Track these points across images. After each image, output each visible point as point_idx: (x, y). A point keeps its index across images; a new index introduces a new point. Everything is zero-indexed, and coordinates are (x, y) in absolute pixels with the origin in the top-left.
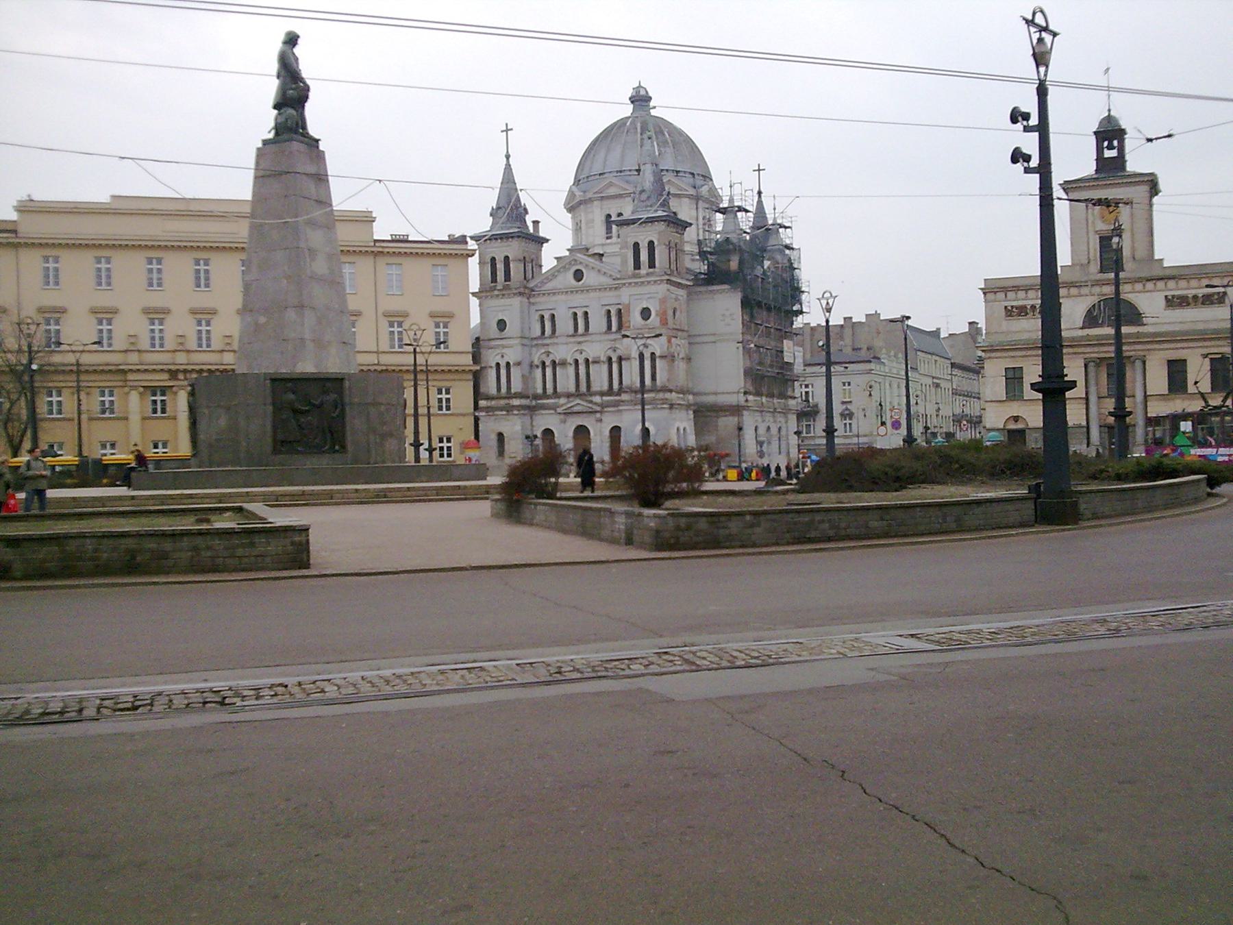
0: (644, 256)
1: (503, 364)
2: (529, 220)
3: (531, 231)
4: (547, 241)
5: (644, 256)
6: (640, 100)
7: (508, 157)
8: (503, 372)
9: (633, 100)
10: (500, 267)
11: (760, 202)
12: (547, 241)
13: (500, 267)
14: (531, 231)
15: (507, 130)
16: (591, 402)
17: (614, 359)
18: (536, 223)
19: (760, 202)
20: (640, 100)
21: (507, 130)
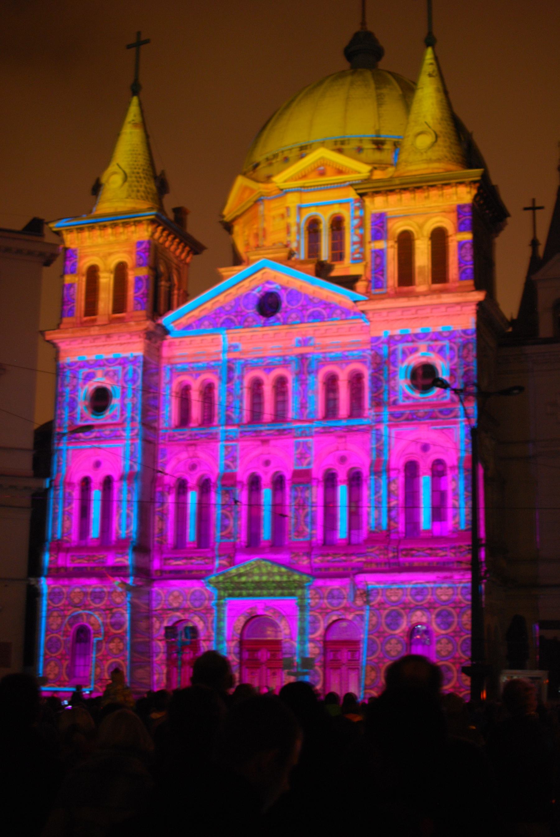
21: (139, 43)
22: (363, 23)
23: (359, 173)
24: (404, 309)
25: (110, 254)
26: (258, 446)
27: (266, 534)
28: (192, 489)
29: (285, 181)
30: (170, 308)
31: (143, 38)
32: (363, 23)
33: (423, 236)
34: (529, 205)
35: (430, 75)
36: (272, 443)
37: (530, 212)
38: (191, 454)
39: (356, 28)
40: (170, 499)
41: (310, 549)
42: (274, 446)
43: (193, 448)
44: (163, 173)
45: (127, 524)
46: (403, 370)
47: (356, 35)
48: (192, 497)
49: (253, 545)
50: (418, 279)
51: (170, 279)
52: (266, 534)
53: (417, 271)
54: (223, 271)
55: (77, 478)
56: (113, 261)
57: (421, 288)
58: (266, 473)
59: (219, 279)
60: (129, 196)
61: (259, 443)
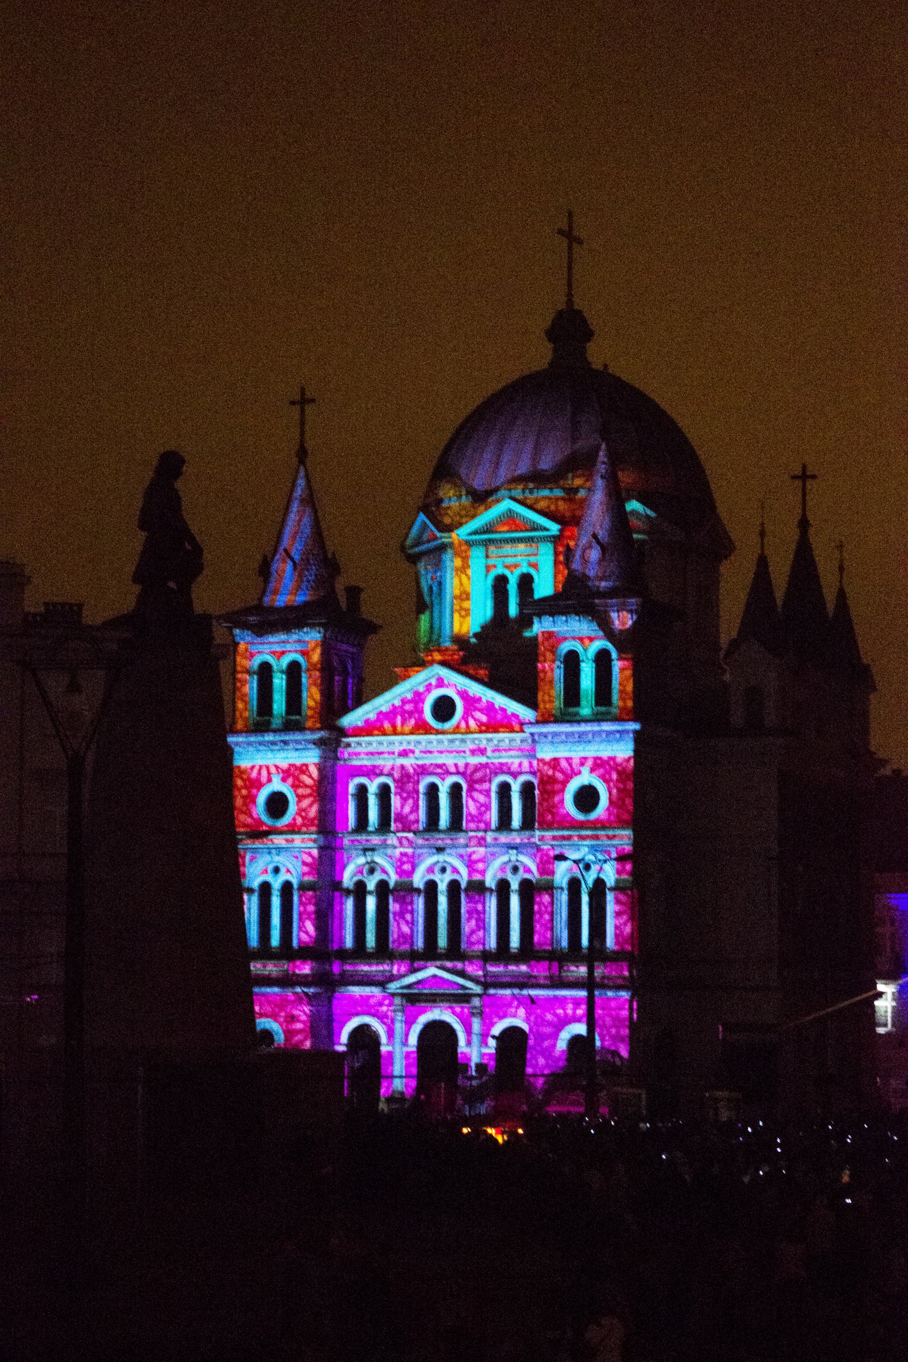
1: (276, 884)
2: (340, 586)
4: (373, 628)
6: (570, 330)
7: (302, 454)
8: (276, 902)
9: (552, 334)
10: (279, 682)
12: (373, 628)
13: (279, 682)
15: (303, 401)
16: (462, 974)
17: (515, 885)
18: (354, 592)
20: (570, 330)
21: (303, 401)
22: (570, 295)
23: (547, 530)
24: (568, 734)
25: (283, 653)
26: (434, 854)
27: (442, 941)
28: (370, 893)
29: (470, 534)
30: (346, 710)
31: (308, 395)
32: (570, 295)
33: (587, 658)
35: (602, 477)
36: (448, 851)
37: (798, 483)
38: (369, 859)
40: (349, 905)
41: (487, 957)
43: (370, 853)
45: (305, 931)
46: (573, 786)
47: (560, 313)
48: (371, 903)
49: (430, 953)
50: (583, 702)
51: (345, 672)
52: (442, 941)
55: (255, 884)
56: (285, 661)
57: (586, 710)
58: (442, 881)
60: (298, 588)
61: (435, 851)
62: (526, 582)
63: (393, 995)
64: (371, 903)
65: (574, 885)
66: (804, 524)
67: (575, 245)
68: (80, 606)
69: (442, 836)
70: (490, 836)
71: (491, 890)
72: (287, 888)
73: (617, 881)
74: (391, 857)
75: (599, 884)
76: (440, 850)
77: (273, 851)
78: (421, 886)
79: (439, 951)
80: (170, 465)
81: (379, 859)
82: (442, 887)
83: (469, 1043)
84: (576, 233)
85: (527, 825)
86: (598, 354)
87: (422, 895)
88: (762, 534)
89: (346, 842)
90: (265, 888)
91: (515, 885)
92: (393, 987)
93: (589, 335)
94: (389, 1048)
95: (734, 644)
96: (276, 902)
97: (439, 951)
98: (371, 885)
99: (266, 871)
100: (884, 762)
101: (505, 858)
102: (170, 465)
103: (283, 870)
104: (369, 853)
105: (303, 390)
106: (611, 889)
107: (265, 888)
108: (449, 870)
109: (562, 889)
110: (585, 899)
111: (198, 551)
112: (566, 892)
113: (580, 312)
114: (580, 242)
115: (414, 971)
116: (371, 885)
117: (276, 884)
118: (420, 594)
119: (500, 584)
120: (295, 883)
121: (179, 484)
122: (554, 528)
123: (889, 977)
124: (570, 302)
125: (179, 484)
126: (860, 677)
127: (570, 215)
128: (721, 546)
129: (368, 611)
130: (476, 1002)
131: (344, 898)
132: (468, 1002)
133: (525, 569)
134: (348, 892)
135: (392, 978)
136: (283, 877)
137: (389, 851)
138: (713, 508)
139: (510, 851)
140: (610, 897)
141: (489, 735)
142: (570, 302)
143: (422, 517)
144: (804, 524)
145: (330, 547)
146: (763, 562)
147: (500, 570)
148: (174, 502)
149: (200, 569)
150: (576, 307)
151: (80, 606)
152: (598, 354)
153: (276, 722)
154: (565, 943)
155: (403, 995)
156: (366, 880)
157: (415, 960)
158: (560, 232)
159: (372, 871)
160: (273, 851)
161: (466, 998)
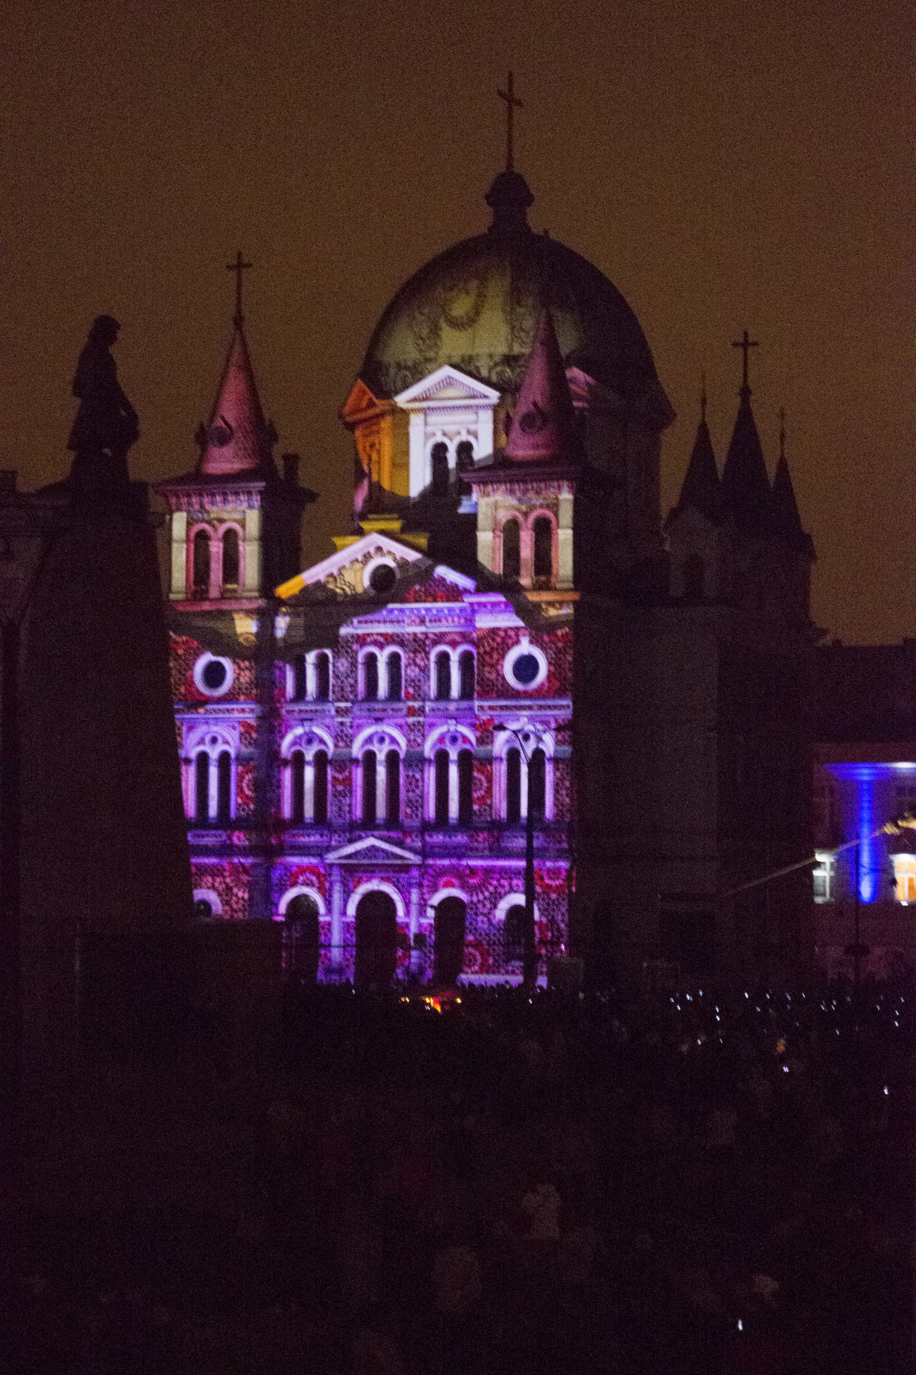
0: (527, 552)
1: (214, 753)
2: (277, 452)
3: (281, 473)
4: (312, 496)
5: (527, 552)
6: (510, 193)
8: (213, 772)
9: (492, 198)
10: (216, 548)
11: (745, 418)
12: (312, 496)
13: (216, 548)
14: (281, 473)
15: (240, 266)
16: (400, 844)
17: (453, 755)
18: (292, 460)
19: (745, 418)
20: (510, 193)
21: (240, 266)
22: (510, 157)
23: (486, 397)
27: (381, 811)
28: (309, 763)
29: (409, 401)
31: (246, 260)
32: (510, 157)
34: (741, 340)
38: (307, 729)
39: (501, 167)
40: (287, 775)
41: (426, 828)
42: (388, 725)
43: (309, 723)
44: (271, 425)
46: (513, 655)
48: (309, 773)
49: (368, 824)
52: (381, 811)
53: (522, 563)
54: (338, 541)
55: (193, 754)
58: (380, 751)
59: (332, 550)
61: (373, 721)
62: (465, 449)
63: (331, 866)
64: (309, 773)
65: (513, 756)
66: (745, 392)
67: (515, 107)
68: (14, 473)
69: (380, 706)
70: (428, 706)
71: (430, 761)
72: (224, 758)
73: (556, 751)
74: (328, 727)
75: (538, 754)
76: (378, 720)
77: (212, 722)
78: (360, 756)
79: (378, 821)
80: (105, 330)
81: (318, 731)
82: (381, 757)
83: (408, 913)
84: (517, 96)
85: (466, 694)
86: (537, 219)
87: (361, 764)
88: (704, 402)
89: (283, 712)
90: (203, 758)
91: (453, 755)
92: (331, 857)
93: (529, 199)
94: (327, 919)
95: (675, 513)
96: (213, 772)
97: (378, 821)
98: (309, 756)
99: (201, 741)
100: (824, 632)
101: (444, 729)
102: (105, 330)
103: (220, 740)
104: (307, 724)
105: (239, 254)
106: (550, 759)
107: (203, 758)
108: (387, 740)
109: (501, 759)
110: (524, 769)
111: (133, 418)
112: (505, 762)
113: (520, 176)
114: (519, 103)
115: (351, 841)
116: (309, 756)
117: (214, 753)
118: (358, 463)
119: (439, 451)
120: (233, 753)
121: (114, 350)
122: (494, 396)
123: (826, 846)
124: (510, 165)
125: (114, 350)
126: (801, 546)
127: (511, 75)
128: (661, 414)
129: (305, 479)
130: (415, 873)
131: (282, 768)
132: (407, 872)
133: (464, 437)
134: (285, 763)
135: (329, 849)
136: (221, 747)
137: (327, 721)
138: (654, 375)
139: (450, 721)
140: (549, 768)
141: (428, 605)
142: (510, 165)
143: (360, 383)
144: (745, 392)
145: (267, 415)
146: (703, 429)
147: (439, 438)
148: (109, 367)
149: (135, 435)
150: (516, 171)
151: (14, 473)
152: (537, 219)
153: (214, 593)
154: (504, 814)
155: (341, 866)
156: (305, 752)
157: (353, 831)
158: (500, 94)
159: (310, 742)
160: (212, 722)
161: (406, 868)
